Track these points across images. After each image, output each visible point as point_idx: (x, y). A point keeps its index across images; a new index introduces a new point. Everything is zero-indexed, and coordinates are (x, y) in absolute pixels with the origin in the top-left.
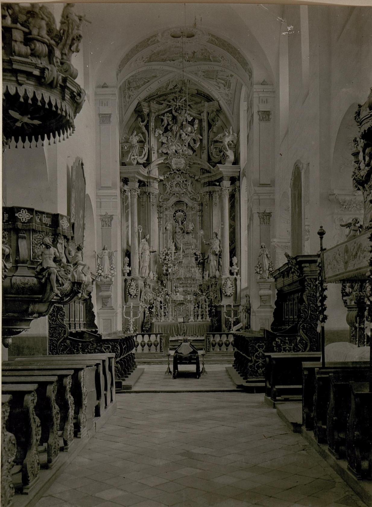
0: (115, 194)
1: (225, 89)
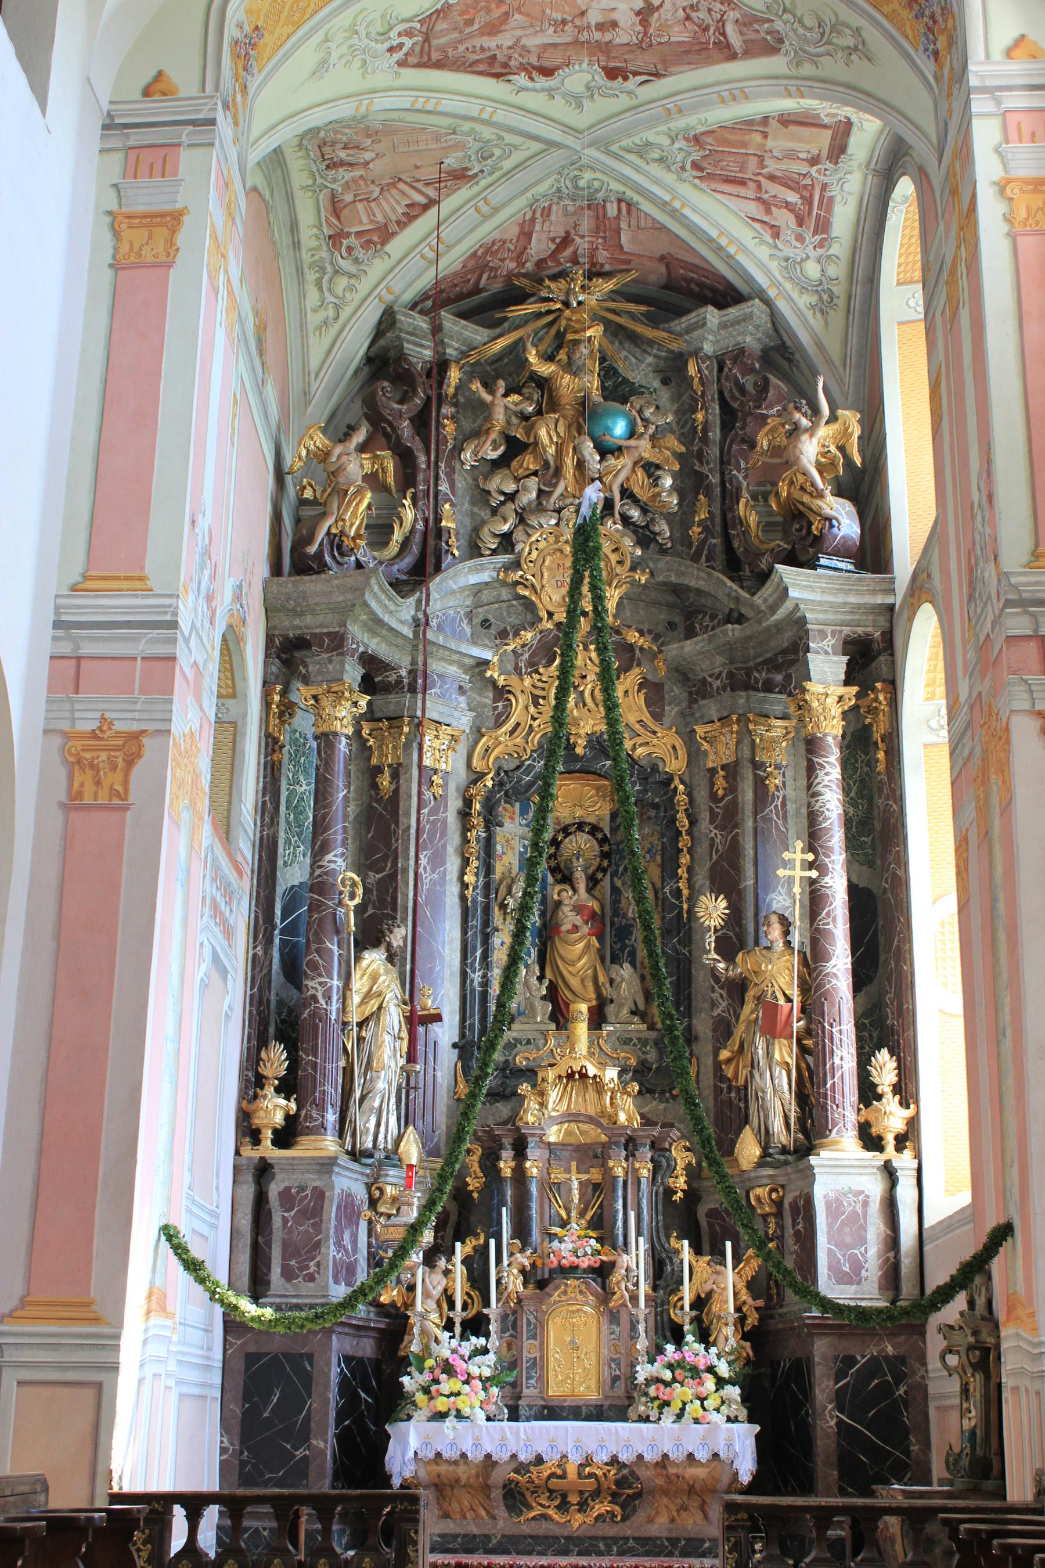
0: (168, 618)
1: (800, 238)
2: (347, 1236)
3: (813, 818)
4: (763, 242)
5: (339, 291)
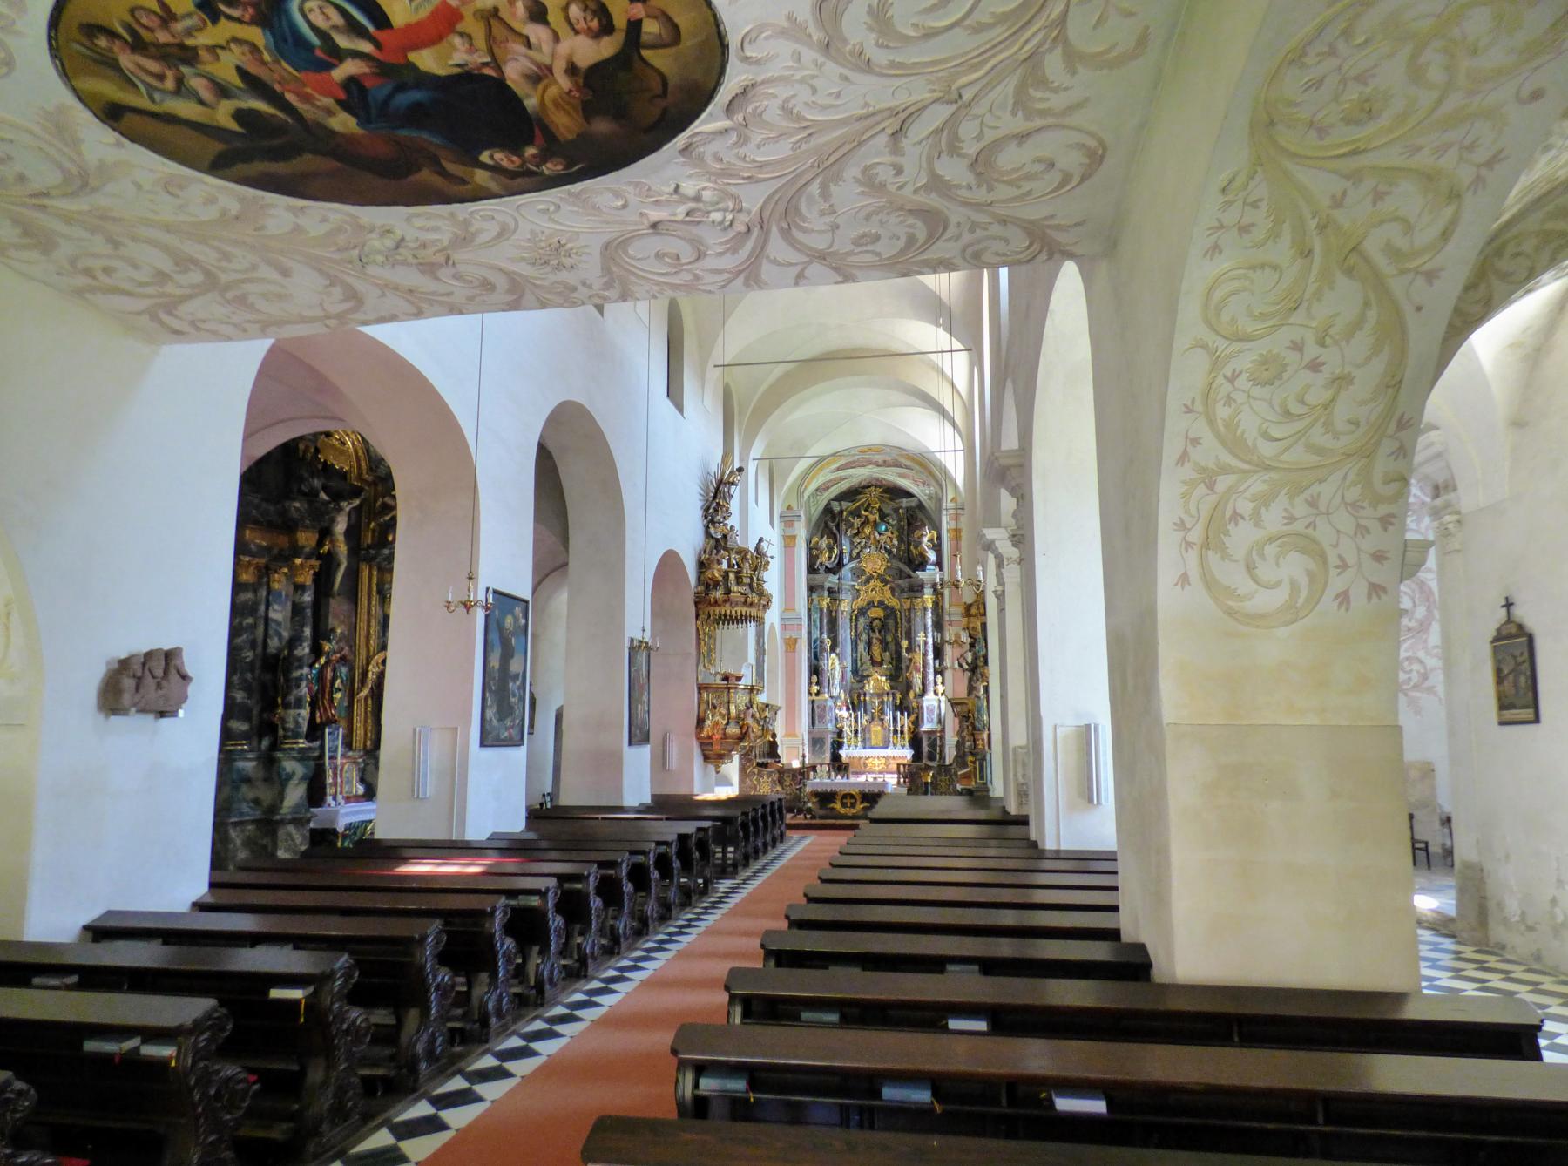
3: (925, 625)
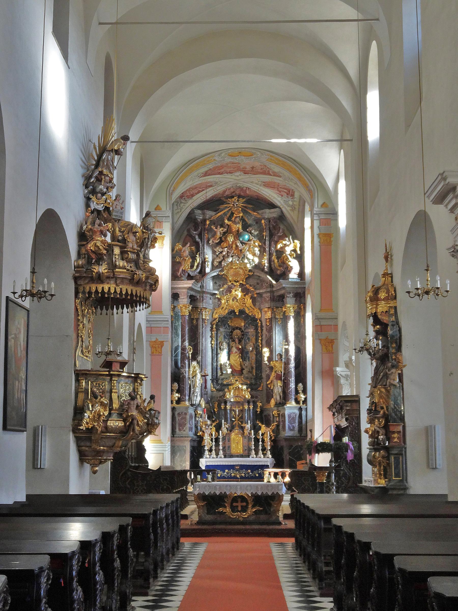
0: (167, 320)
2: (191, 422)
4: (279, 197)
5: (181, 206)
